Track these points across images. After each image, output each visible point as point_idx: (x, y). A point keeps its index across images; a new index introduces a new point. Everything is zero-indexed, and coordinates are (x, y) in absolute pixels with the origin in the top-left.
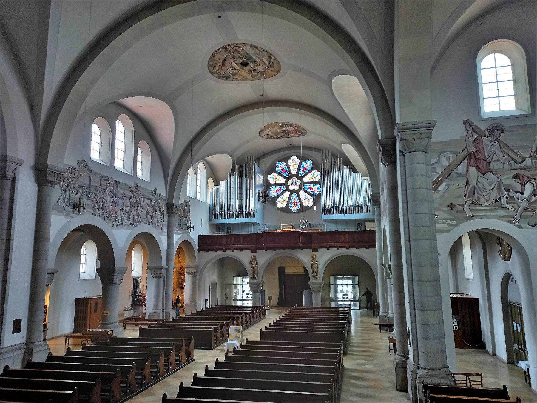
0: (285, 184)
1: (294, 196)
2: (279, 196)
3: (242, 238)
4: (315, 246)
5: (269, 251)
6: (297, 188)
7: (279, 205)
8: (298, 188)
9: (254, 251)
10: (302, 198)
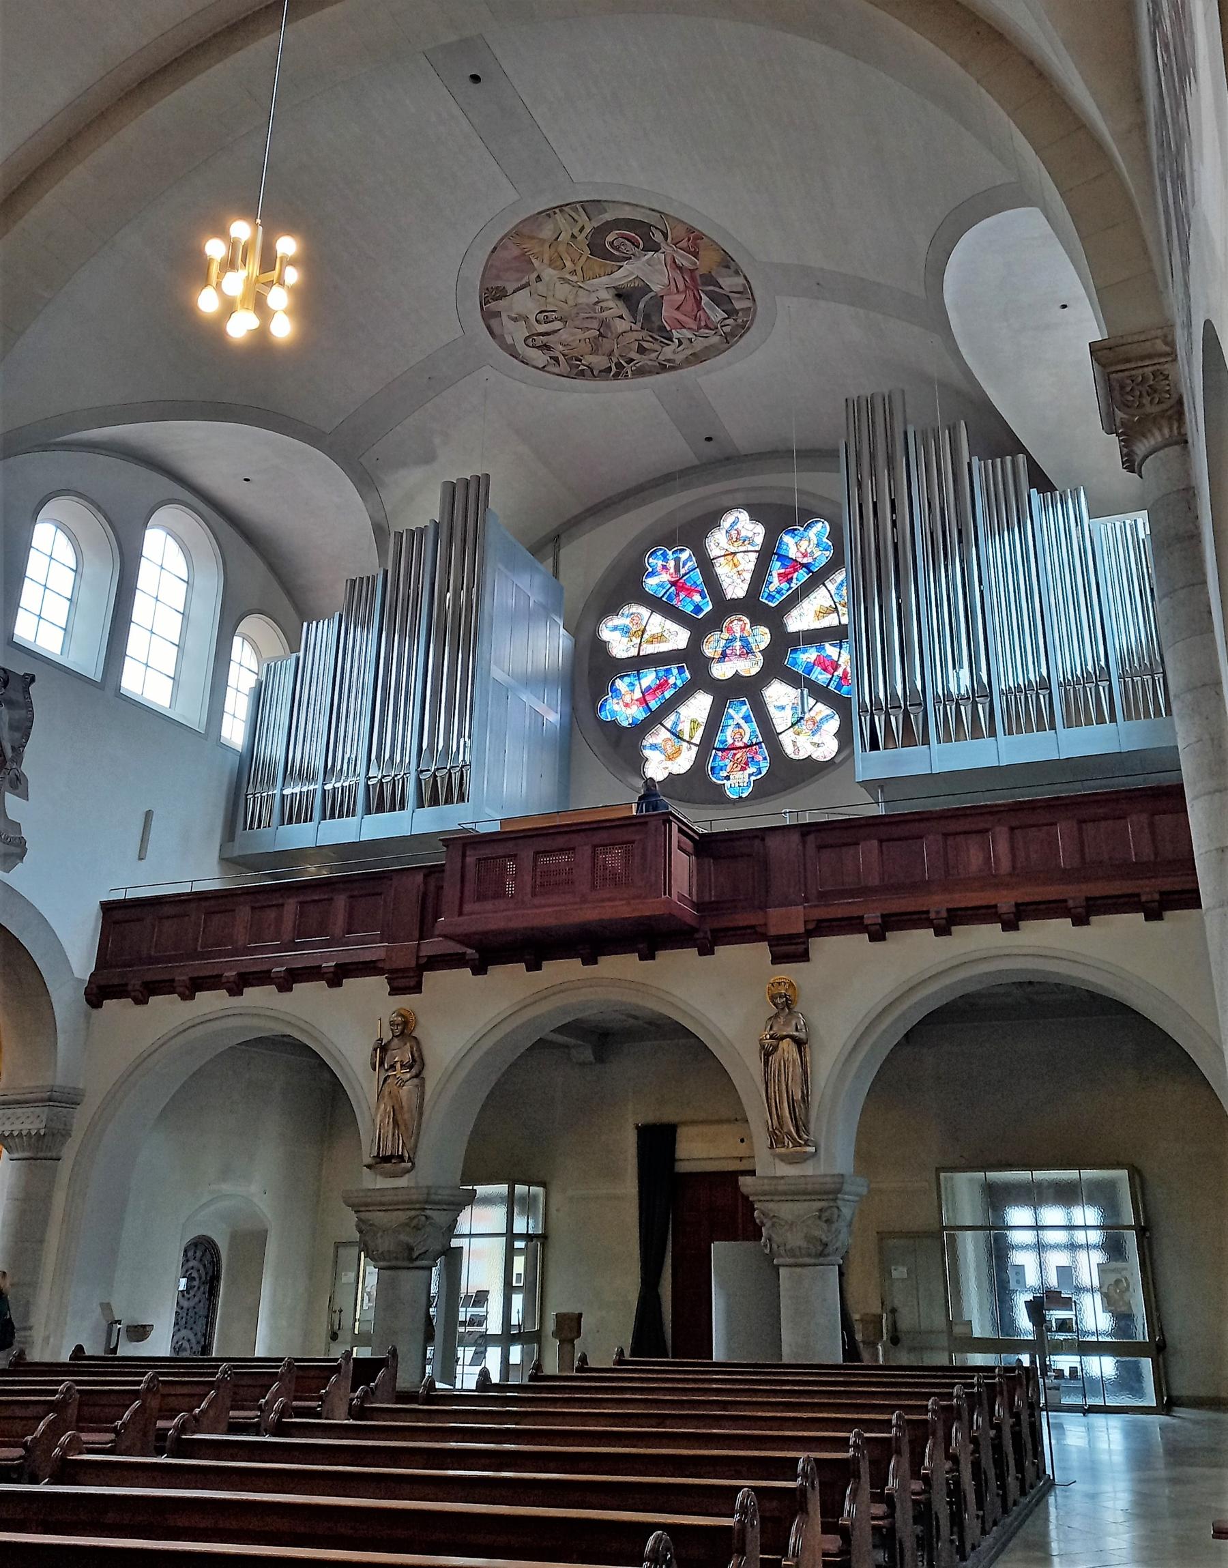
0: (692, 657)
1: (738, 713)
2: (655, 719)
3: (341, 902)
4: (788, 919)
5: (498, 973)
6: (749, 667)
7: (657, 768)
8: (755, 670)
9: (405, 981)
10: (781, 720)
